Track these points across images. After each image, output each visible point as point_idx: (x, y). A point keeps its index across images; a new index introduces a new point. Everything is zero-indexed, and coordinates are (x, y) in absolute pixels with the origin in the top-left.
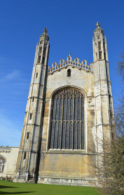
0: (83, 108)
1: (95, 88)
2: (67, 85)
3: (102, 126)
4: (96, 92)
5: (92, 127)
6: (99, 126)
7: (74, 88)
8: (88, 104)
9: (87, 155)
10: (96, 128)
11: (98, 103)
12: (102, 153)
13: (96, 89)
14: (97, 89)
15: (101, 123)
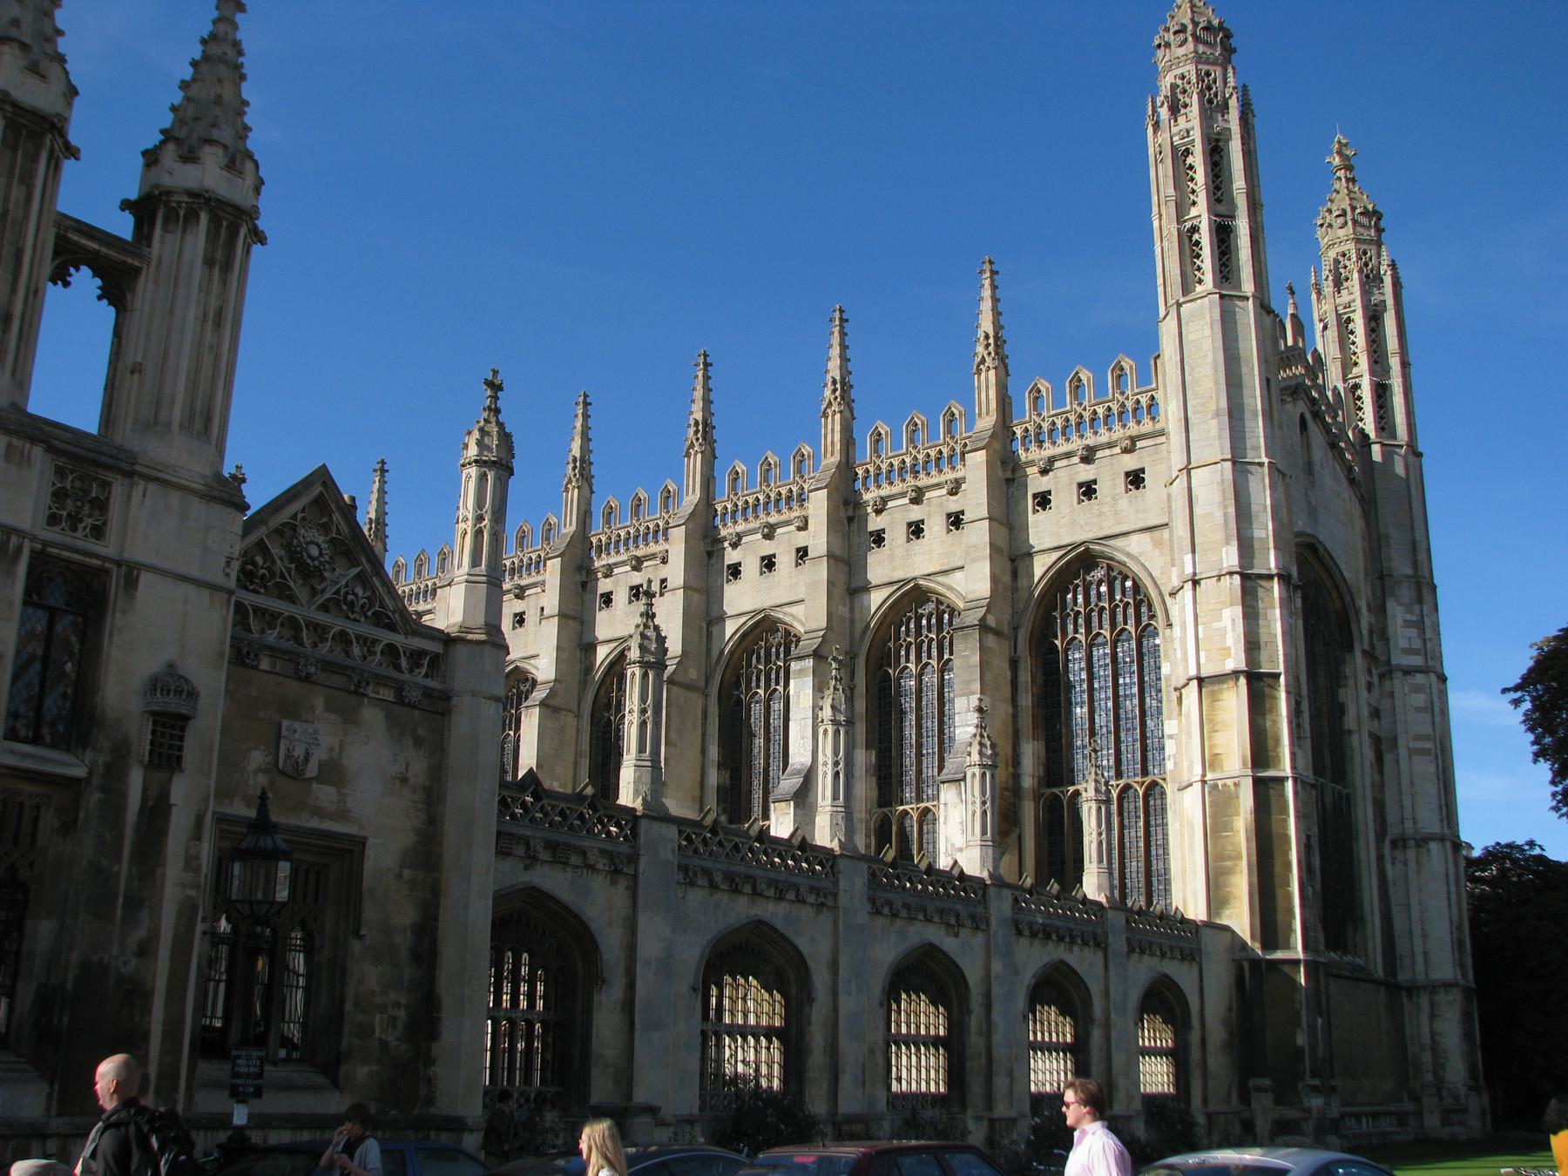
0: (1341, 710)
1: (1397, 614)
2: (1309, 531)
3: (1448, 844)
4: (1403, 643)
5: (1383, 842)
6: (1433, 846)
7: (1320, 560)
8: (1364, 693)
9: (1383, 989)
10: (1418, 845)
11: (1418, 710)
12: (1456, 985)
13: (1400, 622)
14: (1408, 624)
15: (1446, 831)
